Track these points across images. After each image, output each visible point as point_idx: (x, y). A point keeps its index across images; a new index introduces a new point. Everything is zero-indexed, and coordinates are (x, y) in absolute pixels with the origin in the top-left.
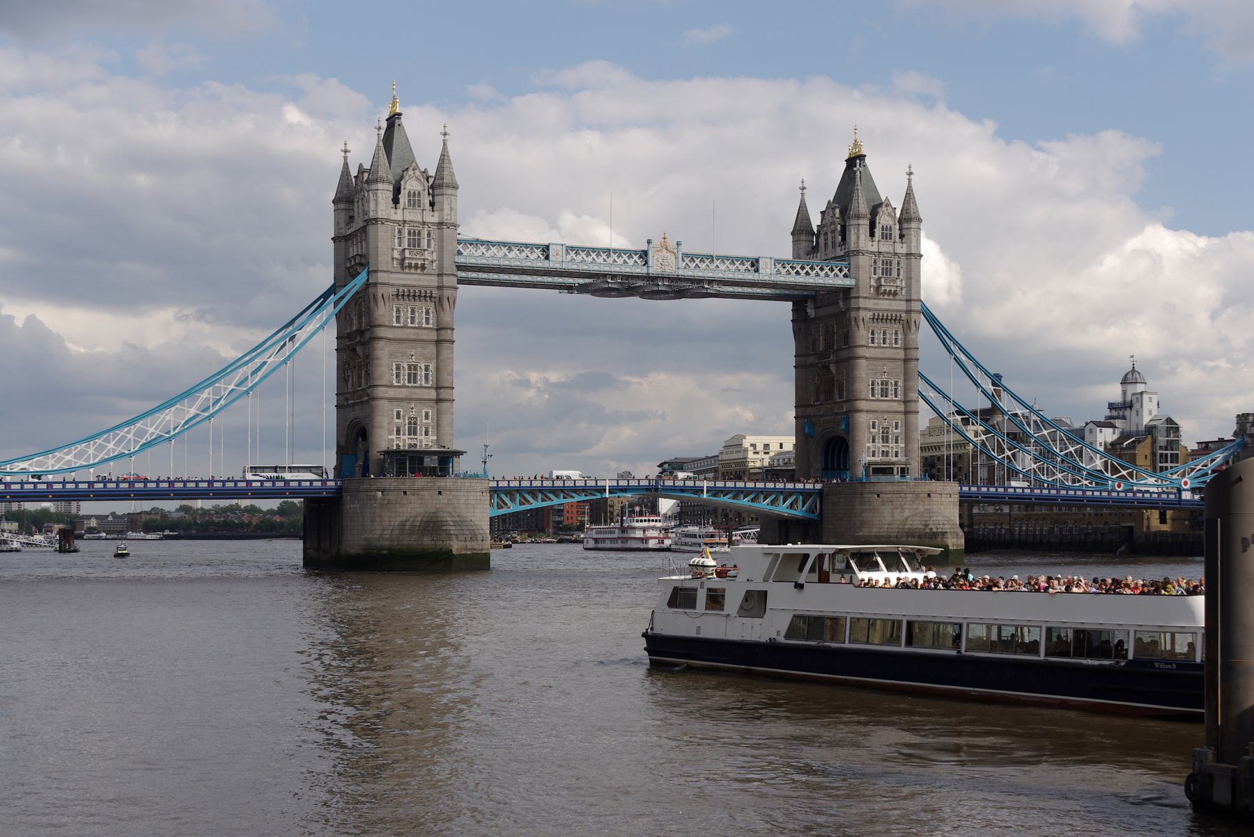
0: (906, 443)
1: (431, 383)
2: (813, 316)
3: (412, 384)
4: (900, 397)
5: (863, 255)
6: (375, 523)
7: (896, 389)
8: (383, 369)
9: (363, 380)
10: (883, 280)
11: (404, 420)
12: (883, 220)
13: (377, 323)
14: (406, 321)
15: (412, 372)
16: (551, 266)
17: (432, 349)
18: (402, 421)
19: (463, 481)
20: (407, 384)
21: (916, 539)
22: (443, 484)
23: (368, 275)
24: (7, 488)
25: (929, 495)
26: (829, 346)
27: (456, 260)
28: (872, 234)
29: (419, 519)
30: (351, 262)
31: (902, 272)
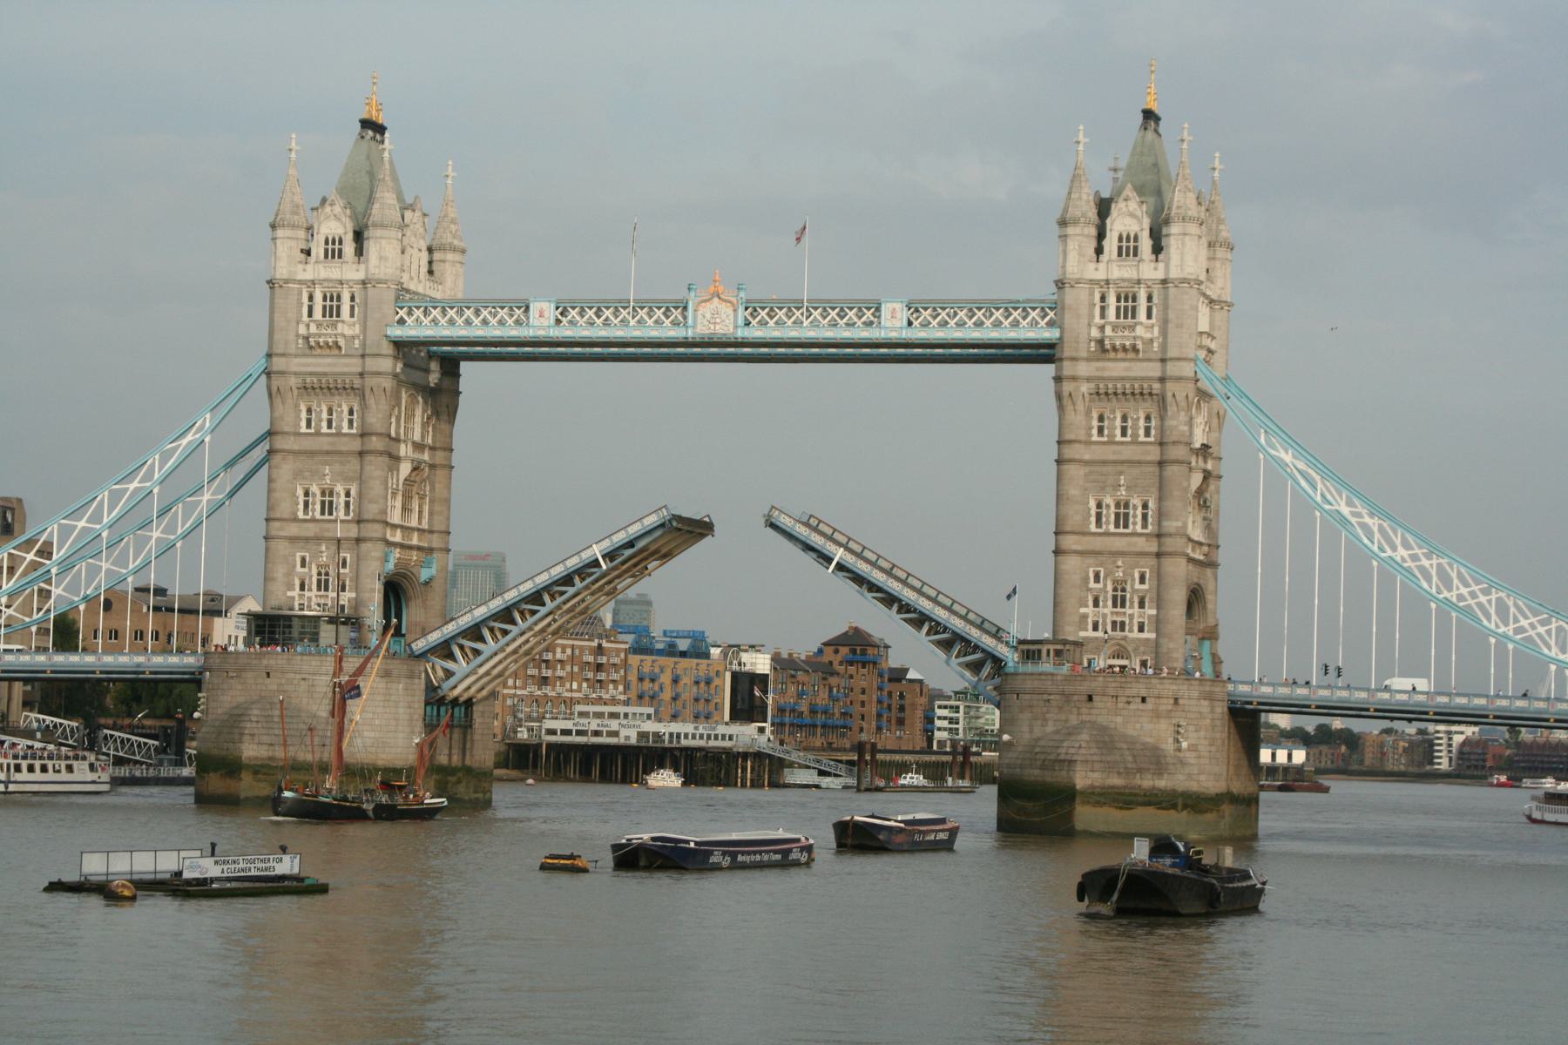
0: (1158, 608)
3: (327, 517)
5: (1072, 287)
7: (1145, 517)
11: (310, 569)
14: (319, 426)
15: (327, 499)
17: (354, 464)
18: (306, 570)
19: (305, 658)
20: (318, 515)
22: (272, 662)
25: (1090, 698)
27: (389, 333)
28: (1099, 251)
31: (1154, 311)
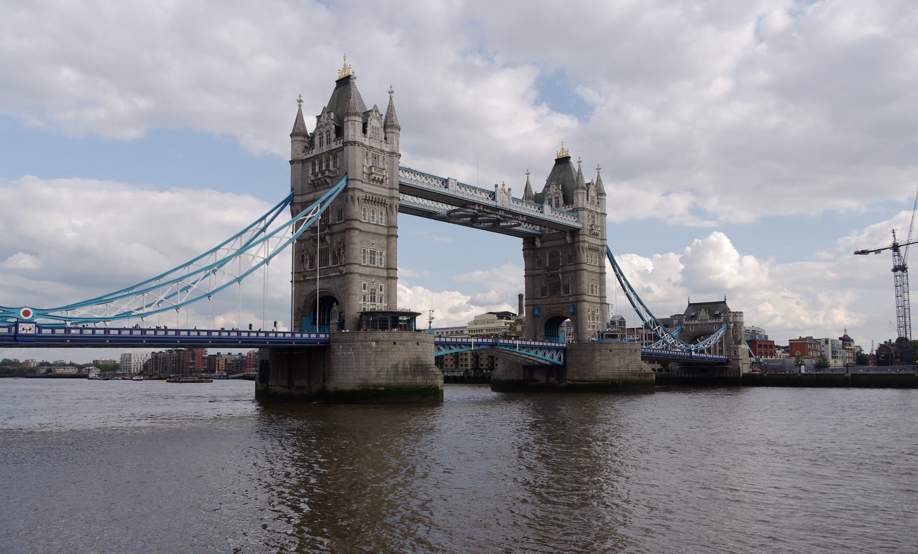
1: (383, 266)
2: (539, 247)
4: (598, 295)
6: (370, 366)
8: (358, 252)
9: (330, 261)
10: (594, 226)
12: (592, 193)
13: (354, 218)
16: (450, 193)
17: (384, 241)
20: (370, 265)
21: (637, 377)
22: (419, 337)
23: (347, 182)
24: (67, 332)
26: (554, 265)
29: (408, 363)
30: (317, 175)
31: (599, 222)
